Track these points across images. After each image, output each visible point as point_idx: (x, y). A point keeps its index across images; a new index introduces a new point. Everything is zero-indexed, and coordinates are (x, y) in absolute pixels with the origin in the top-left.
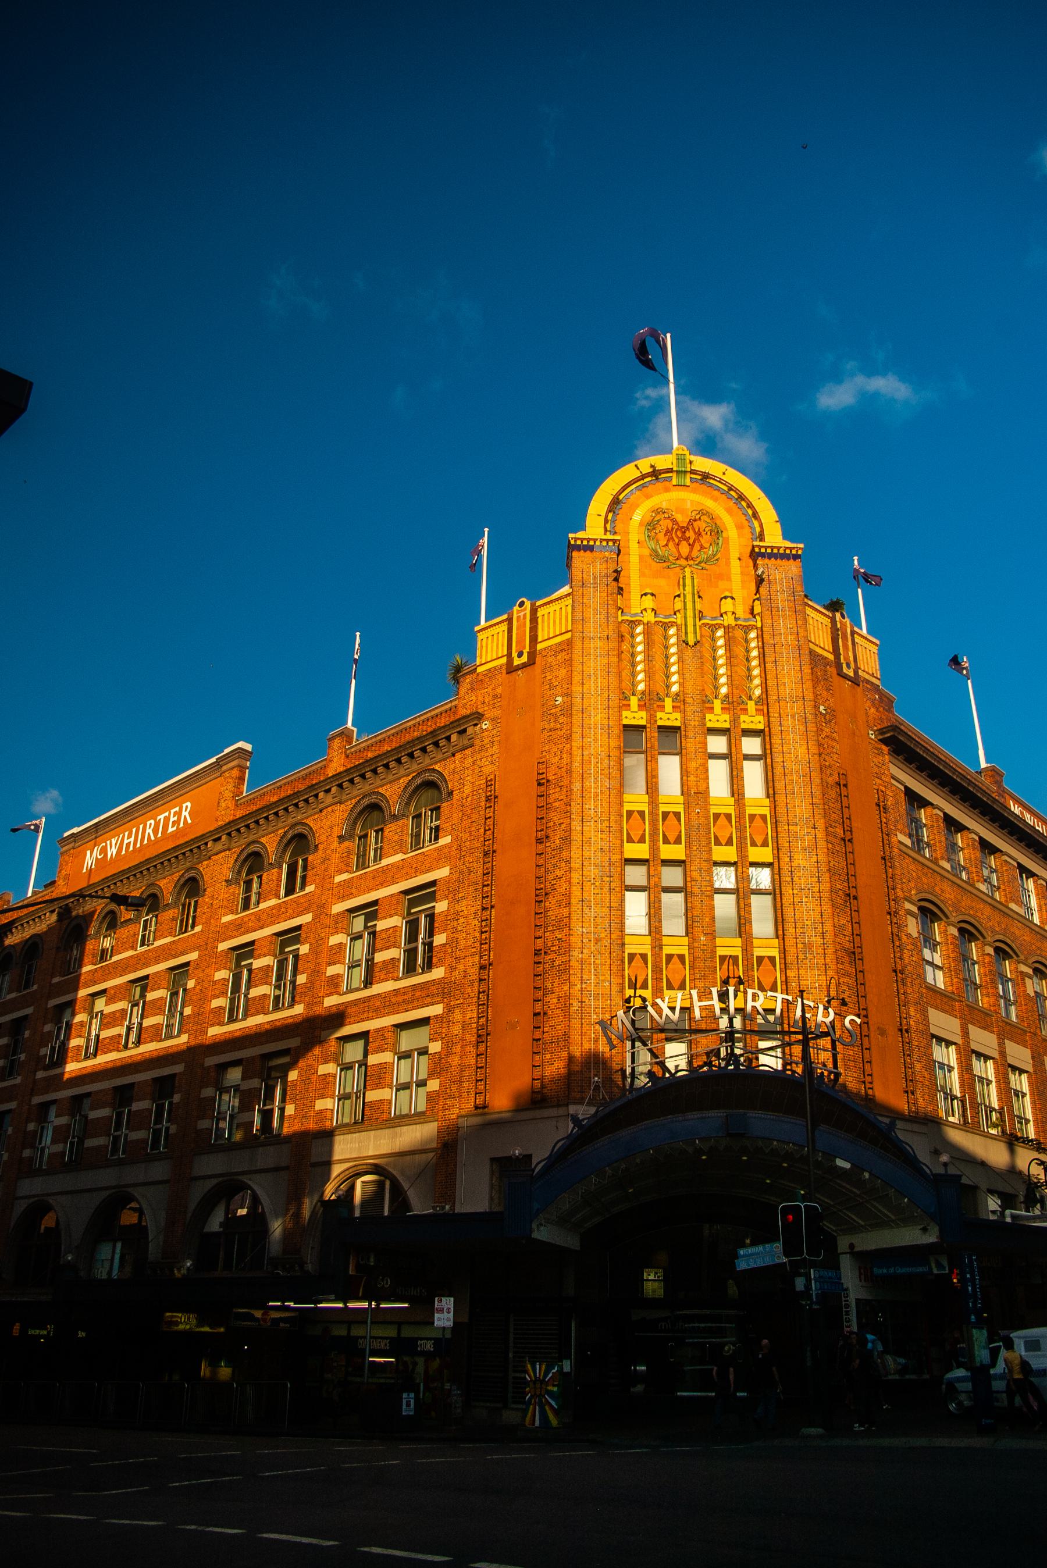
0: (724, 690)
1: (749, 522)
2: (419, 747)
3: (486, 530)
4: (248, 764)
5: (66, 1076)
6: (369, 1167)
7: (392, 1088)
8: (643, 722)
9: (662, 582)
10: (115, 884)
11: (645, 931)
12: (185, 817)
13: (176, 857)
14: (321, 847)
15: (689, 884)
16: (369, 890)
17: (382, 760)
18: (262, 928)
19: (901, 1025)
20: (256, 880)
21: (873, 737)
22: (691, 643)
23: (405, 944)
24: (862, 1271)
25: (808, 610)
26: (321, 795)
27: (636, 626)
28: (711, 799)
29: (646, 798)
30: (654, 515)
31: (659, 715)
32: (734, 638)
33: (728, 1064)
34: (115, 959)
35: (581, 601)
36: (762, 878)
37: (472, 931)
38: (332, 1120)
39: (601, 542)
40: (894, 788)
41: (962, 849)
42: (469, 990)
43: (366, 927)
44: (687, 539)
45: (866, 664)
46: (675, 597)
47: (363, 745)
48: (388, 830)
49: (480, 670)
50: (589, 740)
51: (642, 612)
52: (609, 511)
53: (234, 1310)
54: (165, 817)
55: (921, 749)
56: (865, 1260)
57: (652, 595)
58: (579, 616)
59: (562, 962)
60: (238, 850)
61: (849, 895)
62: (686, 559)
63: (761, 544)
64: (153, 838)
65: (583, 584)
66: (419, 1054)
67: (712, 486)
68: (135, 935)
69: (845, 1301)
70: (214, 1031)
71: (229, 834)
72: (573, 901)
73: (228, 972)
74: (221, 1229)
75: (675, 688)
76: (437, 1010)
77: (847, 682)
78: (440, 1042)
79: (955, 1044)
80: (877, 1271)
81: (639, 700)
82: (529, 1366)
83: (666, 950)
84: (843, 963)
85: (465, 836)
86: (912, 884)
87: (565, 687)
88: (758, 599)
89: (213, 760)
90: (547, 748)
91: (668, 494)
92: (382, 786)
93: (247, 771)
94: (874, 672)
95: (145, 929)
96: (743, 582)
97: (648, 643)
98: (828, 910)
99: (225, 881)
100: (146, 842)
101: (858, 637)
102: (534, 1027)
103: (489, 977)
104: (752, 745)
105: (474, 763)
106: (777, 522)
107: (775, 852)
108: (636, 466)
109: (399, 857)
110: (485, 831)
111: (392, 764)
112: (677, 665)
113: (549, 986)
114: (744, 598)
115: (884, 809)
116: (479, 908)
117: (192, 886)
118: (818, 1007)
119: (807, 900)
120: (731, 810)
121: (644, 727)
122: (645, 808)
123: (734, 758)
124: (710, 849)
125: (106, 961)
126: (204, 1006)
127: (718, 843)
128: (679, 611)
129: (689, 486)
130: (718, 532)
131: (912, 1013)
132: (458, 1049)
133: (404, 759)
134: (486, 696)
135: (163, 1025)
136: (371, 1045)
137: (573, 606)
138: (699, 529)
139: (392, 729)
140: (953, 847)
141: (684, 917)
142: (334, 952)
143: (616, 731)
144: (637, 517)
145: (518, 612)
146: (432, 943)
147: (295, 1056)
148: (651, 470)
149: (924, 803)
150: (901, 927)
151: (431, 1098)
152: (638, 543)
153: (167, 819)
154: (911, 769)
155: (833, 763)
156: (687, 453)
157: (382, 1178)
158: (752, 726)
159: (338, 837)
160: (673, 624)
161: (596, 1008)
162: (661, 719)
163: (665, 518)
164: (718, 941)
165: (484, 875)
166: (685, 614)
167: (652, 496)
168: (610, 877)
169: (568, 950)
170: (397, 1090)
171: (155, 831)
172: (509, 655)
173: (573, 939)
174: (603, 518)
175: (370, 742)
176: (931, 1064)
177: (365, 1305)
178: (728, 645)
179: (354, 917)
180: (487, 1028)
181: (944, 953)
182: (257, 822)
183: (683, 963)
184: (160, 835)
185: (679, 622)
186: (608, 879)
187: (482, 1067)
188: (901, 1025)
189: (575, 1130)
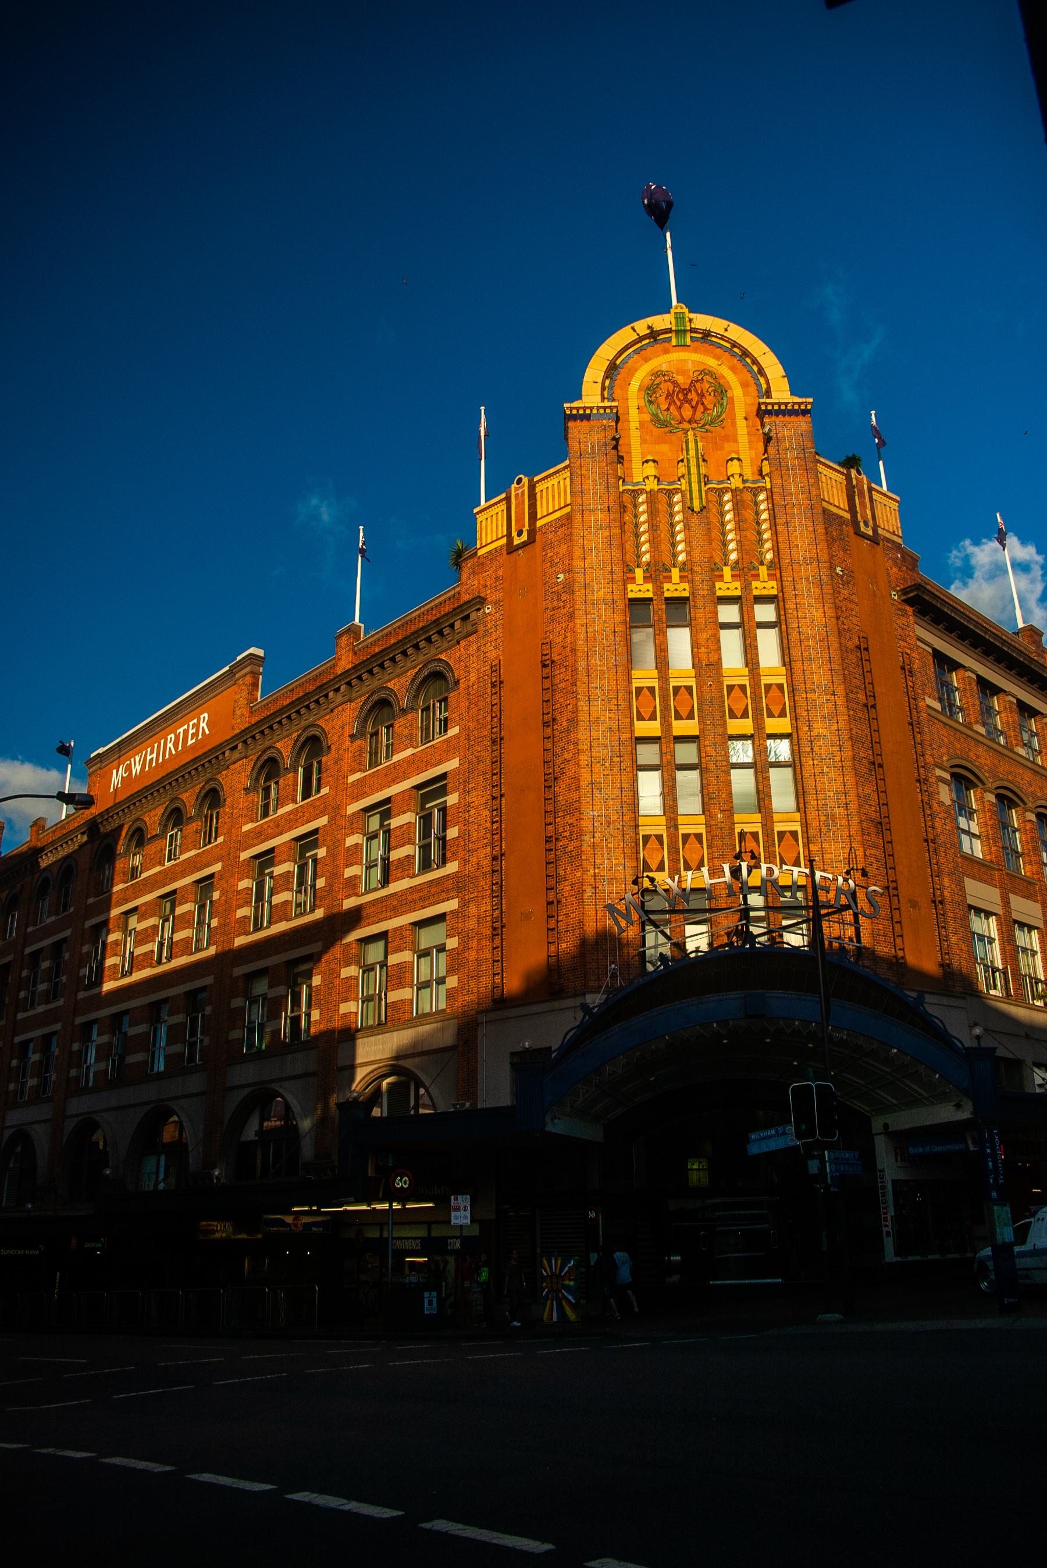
0: (733, 556)
1: (754, 379)
3: (483, 408)
4: (261, 669)
5: (103, 993)
6: (388, 1068)
7: (412, 988)
8: (650, 595)
9: (665, 448)
10: (140, 801)
11: (659, 811)
13: (196, 769)
14: (333, 748)
15: (704, 760)
16: (382, 788)
17: (388, 654)
18: (281, 834)
19: (934, 896)
20: (273, 786)
21: (896, 598)
22: (697, 509)
23: (420, 840)
24: (898, 1151)
25: (821, 468)
26: (331, 695)
27: (639, 495)
28: (724, 670)
29: (655, 674)
30: (653, 378)
31: (666, 586)
32: (742, 501)
33: (744, 944)
34: (144, 875)
35: (580, 473)
36: (782, 750)
37: (483, 822)
38: (356, 1022)
39: (598, 410)
40: (921, 651)
41: (999, 713)
42: (483, 883)
43: (382, 825)
44: (689, 402)
45: (885, 522)
46: (678, 462)
47: (370, 641)
48: (398, 725)
49: (480, 553)
50: (593, 616)
51: (644, 481)
52: (606, 377)
53: (265, 1216)
54: (184, 730)
55: (948, 608)
56: (901, 1139)
57: (654, 461)
58: (578, 488)
59: (574, 848)
60: (254, 757)
61: (873, 763)
62: (690, 422)
63: (768, 401)
64: (174, 752)
65: (581, 455)
66: (438, 951)
67: (713, 344)
68: (162, 850)
69: (881, 1182)
70: (240, 941)
71: (245, 742)
72: (583, 784)
73: (251, 881)
74: (257, 1138)
75: (682, 558)
76: (452, 905)
78: (457, 937)
79: (995, 914)
80: (912, 1150)
81: (644, 572)
82: (545, 1261)
83: (683, 830)
84: (869, 834)
85: (472, 725)
86: (944, 750)
87: (567, 563)
88: (766, 459)
89: (227, 668)
90: (551, 628)
91: (667, 355)
92: (390, 681)
93: (261, 676)
94: (895, 530)
95: (171, 845)
96: (750, 442)
97: (652, 512)
98: (850, 779)
99: (244, 789)
100: (167, 756)
101: (876, 493)
102: (548, 917)
103: (501, 868)
104: (765, 613)
105: (478, 648)
106: (784, 377)
107: (794, 722)
108: (633, 328)
109: (409, 752)
110: (492, 718)
111: (398, 658)
112: (683, 533)
113: (562, 873)
114: (751, 460)
115: (910, 672)
116: (489, 797)
117: (213, 797)
118: (837, 880)
119: (828, 770)
120: (746, 681)
121: (650, 599)
122: (655, 684)
123: (747, 628)
124: (725, 723)
125: (136, 878)
126: (229, 916)
127: (733, 715)
128: (683, 476)
129: (689, 346)
130: (722, 391)
131: (947, 884)
132: (474, 944)
133: (410, 651)
135: (192, 938)
136: (390, 945)
137: (571, 478)
138: (702, 390)
139: (397, 621)
140: (988, 712)
141: (700, 795)
142: (351, 853)
144: (635, 385)
145: (516, 489)
146: (445, 837)
147: (314, 958)
148: (648, 331)
149: (955, 666)
150: (931, 795)
151: (451, 994)
152: (638, 409)
153: (186, 732)
154: (939, 630)
155: (852, 626)
156: (686, 310)
157: (403, 1078)
158: (765, 592)
159: (349, 736)
160: (677, 491)
161: (611, 893)
162: (668, 590)
163: (665, 381)
164: (737, 818)
165: (493, 763)
166: (690, 479)
167: (650, 359)
168: (620, 757)
169: (580, 833)
170: (418, 989)
171: (176, 745)
172: (509, 535)
173: (583, 823)
174: (599, 385)
175: (377, 636)
176: (971, 937)
177: (386, 1206)
178: (736, 509)
179: (369, 817)
180: (502, 921)
181: (982, 820)
182: (271, 727)
183: (701, 842)
184: (180, 748)
185: (683, 488)
186: (618, 759)
187: (498, 961)
188: (934, 896)
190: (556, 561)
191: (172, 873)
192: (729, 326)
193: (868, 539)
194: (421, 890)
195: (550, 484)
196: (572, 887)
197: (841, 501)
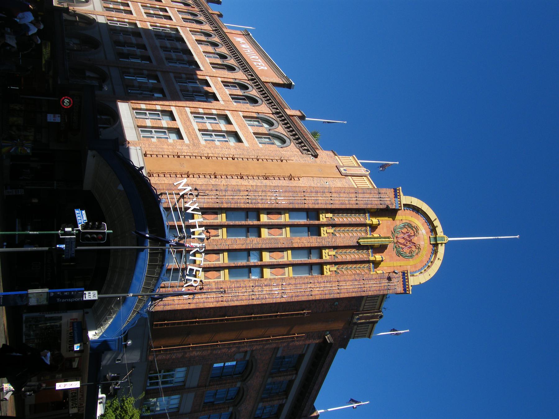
3: (398, 163)
9: (385, 230)
12: (260, 67)
18: (217, 89)
22: (359, 240)
39: (399, 201)
46: (379, 234)
63: (409, 274)
64: (251, 58)
77: (350, 319)
89: (286, 76)
106: (420, 283)
108: (436, 219)
134: (325, 159)
143: (317, 206)
153: (259, 62)
156: (445, 242)
163: (414, 232)
167: (423, 226)
171: (253, 59)
184: (252, 60)
189: (137, 168)
190: (334, 182)
191: (200, 55)
192: (440, 260)
193: (351, 321)
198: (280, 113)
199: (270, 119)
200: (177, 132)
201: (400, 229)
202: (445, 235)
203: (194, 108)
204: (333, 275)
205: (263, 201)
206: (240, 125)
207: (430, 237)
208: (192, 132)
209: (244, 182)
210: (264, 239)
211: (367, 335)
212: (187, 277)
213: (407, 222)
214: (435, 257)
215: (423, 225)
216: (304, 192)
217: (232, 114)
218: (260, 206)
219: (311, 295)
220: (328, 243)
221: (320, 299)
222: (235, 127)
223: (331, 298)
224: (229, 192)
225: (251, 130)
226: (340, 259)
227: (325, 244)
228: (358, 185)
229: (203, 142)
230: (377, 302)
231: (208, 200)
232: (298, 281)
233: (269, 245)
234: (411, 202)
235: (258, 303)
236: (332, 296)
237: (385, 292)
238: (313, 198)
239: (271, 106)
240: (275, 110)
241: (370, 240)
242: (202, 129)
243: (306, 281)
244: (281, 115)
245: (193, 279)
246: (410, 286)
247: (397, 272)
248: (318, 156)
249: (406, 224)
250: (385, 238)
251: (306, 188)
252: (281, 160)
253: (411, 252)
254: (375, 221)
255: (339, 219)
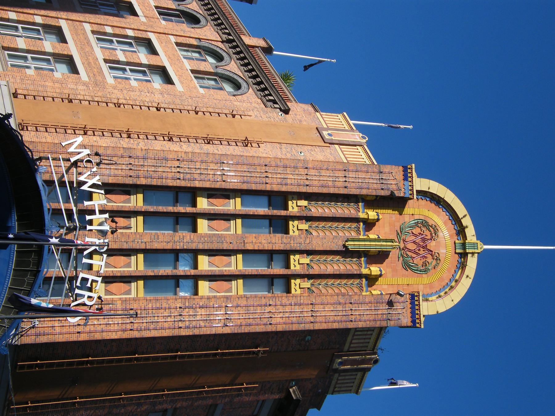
2: (263, 80)
3: (411, 127)
9: (387, 229)
22: (347, 243)
39: (410, 186)
46: (378, 235)
63: (421, 298)
77: (329, 363)
85: (206, 100)
106: (437, 312)
139: (274, 71)
143: (284, 189)
156: (479, 251)
163: (431, 234)
190: (312, 153)
192: (470, 278)
193: (330, 365)
194: (95, 64)
195: (362, 153)
196: (95, 141)
197: (355, 345)
198: (233, 41)
199: (218, 50)
200: (69, 61)
201: (409, 229)
202: (479, 241)
203: (97, 24)
204: (305, 295)
205: (203, 177)
206: (170, 56)
207: (455, 243)
208: (93, 63)
209: (173, 147)
210: (201, 236)
211: (354, 389)
212: (77, 291)
213: (420, 218)
214: (461, 273)
215: (445, 223)
216: (266, 165)
217: (159, 39)
218: (197, 184)
219: (270, 324)
220: (298, 245)
221: (284, 330)
222: (163, 60)
223: (300, 329)
224: (149, 161)
225: (188, 65)
226: (316, 270)
227: (294, 246)
228: (348, 159)
229: (110, 80)
230: (370, 338)
231: (116, 172)
232: (250, 302)
233: (209, 244)
234: (429, 188)
235: (187, 334)
236: (301, 327)
237: (384, 324)
238: (279, 176)
239: (220, 30)
240: (226, 36)
241: (363, 243)
242: (110, 60)
243: (263, 301)
244: (234, 44)
245: (87, 294)
246: (422, 316)
247: (403, 294)
248: (290, 112)
249: (419, 221)
250: (386, 241)
251: (269, 160)
252: (232, 115)
253: (425, 264)
254: (372, 214)
255: (317, 209)
